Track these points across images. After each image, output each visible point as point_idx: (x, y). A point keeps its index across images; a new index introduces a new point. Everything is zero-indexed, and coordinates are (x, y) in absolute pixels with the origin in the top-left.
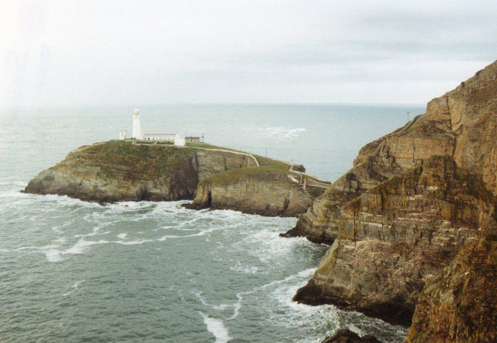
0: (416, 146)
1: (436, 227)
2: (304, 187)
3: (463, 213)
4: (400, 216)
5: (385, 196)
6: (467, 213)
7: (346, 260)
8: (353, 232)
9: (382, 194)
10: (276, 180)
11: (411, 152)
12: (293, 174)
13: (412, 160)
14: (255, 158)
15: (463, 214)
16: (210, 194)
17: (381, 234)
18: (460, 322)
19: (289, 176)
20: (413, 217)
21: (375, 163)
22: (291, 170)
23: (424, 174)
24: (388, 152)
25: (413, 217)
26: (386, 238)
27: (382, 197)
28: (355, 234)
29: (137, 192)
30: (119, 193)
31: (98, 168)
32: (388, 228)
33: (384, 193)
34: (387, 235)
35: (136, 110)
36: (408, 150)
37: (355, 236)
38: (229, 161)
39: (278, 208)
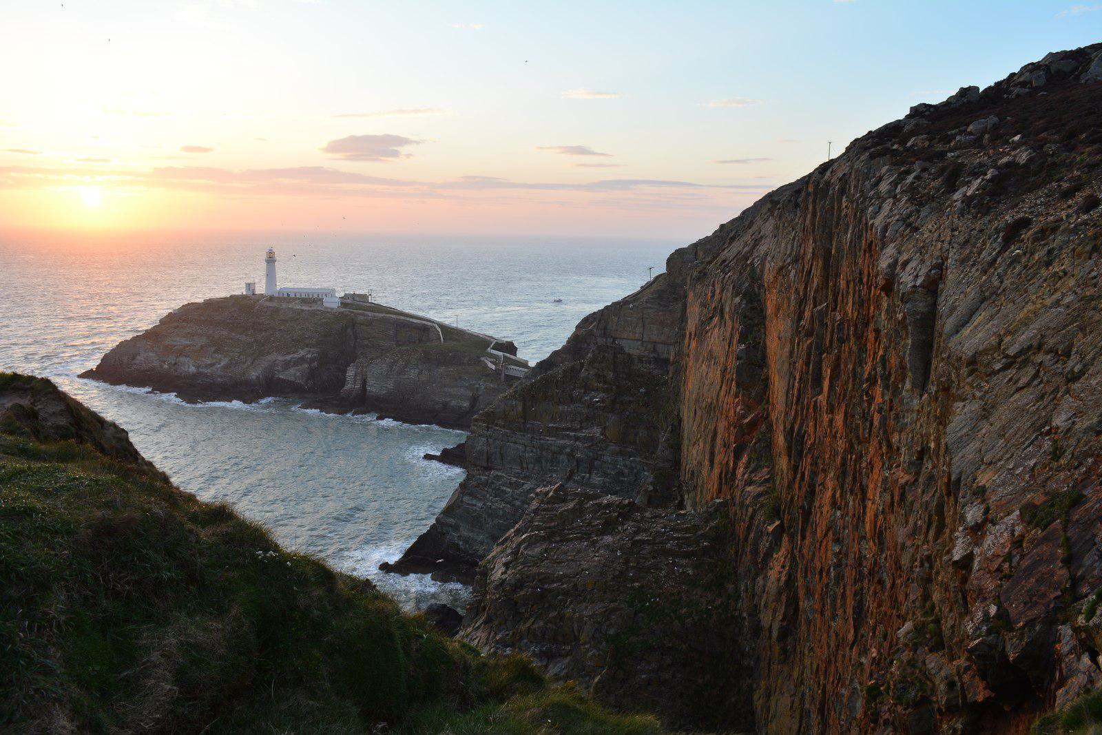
1: (599, 453)
4: (549, 436)
6: (642, 433)
7: (476, 497)
8: (485, 457)
11: (639, 330)
12: (491, 356)
13: (640, 343)
14: (439, 329)
16: (364, 383)
17: (523, 460)
18: (501, 609)
19: (482, 359)
20: (568, 437)
21: (586, 345)
23: (584, 373)
24: (605, 329)
25: (568, 437)
26: (531, 466)
28: (488, 459)
30: (231, 377)
32: (532, 451)
34: (531, 463)
36: (635, 327)
37: (487, 461)
39: (460, 407)
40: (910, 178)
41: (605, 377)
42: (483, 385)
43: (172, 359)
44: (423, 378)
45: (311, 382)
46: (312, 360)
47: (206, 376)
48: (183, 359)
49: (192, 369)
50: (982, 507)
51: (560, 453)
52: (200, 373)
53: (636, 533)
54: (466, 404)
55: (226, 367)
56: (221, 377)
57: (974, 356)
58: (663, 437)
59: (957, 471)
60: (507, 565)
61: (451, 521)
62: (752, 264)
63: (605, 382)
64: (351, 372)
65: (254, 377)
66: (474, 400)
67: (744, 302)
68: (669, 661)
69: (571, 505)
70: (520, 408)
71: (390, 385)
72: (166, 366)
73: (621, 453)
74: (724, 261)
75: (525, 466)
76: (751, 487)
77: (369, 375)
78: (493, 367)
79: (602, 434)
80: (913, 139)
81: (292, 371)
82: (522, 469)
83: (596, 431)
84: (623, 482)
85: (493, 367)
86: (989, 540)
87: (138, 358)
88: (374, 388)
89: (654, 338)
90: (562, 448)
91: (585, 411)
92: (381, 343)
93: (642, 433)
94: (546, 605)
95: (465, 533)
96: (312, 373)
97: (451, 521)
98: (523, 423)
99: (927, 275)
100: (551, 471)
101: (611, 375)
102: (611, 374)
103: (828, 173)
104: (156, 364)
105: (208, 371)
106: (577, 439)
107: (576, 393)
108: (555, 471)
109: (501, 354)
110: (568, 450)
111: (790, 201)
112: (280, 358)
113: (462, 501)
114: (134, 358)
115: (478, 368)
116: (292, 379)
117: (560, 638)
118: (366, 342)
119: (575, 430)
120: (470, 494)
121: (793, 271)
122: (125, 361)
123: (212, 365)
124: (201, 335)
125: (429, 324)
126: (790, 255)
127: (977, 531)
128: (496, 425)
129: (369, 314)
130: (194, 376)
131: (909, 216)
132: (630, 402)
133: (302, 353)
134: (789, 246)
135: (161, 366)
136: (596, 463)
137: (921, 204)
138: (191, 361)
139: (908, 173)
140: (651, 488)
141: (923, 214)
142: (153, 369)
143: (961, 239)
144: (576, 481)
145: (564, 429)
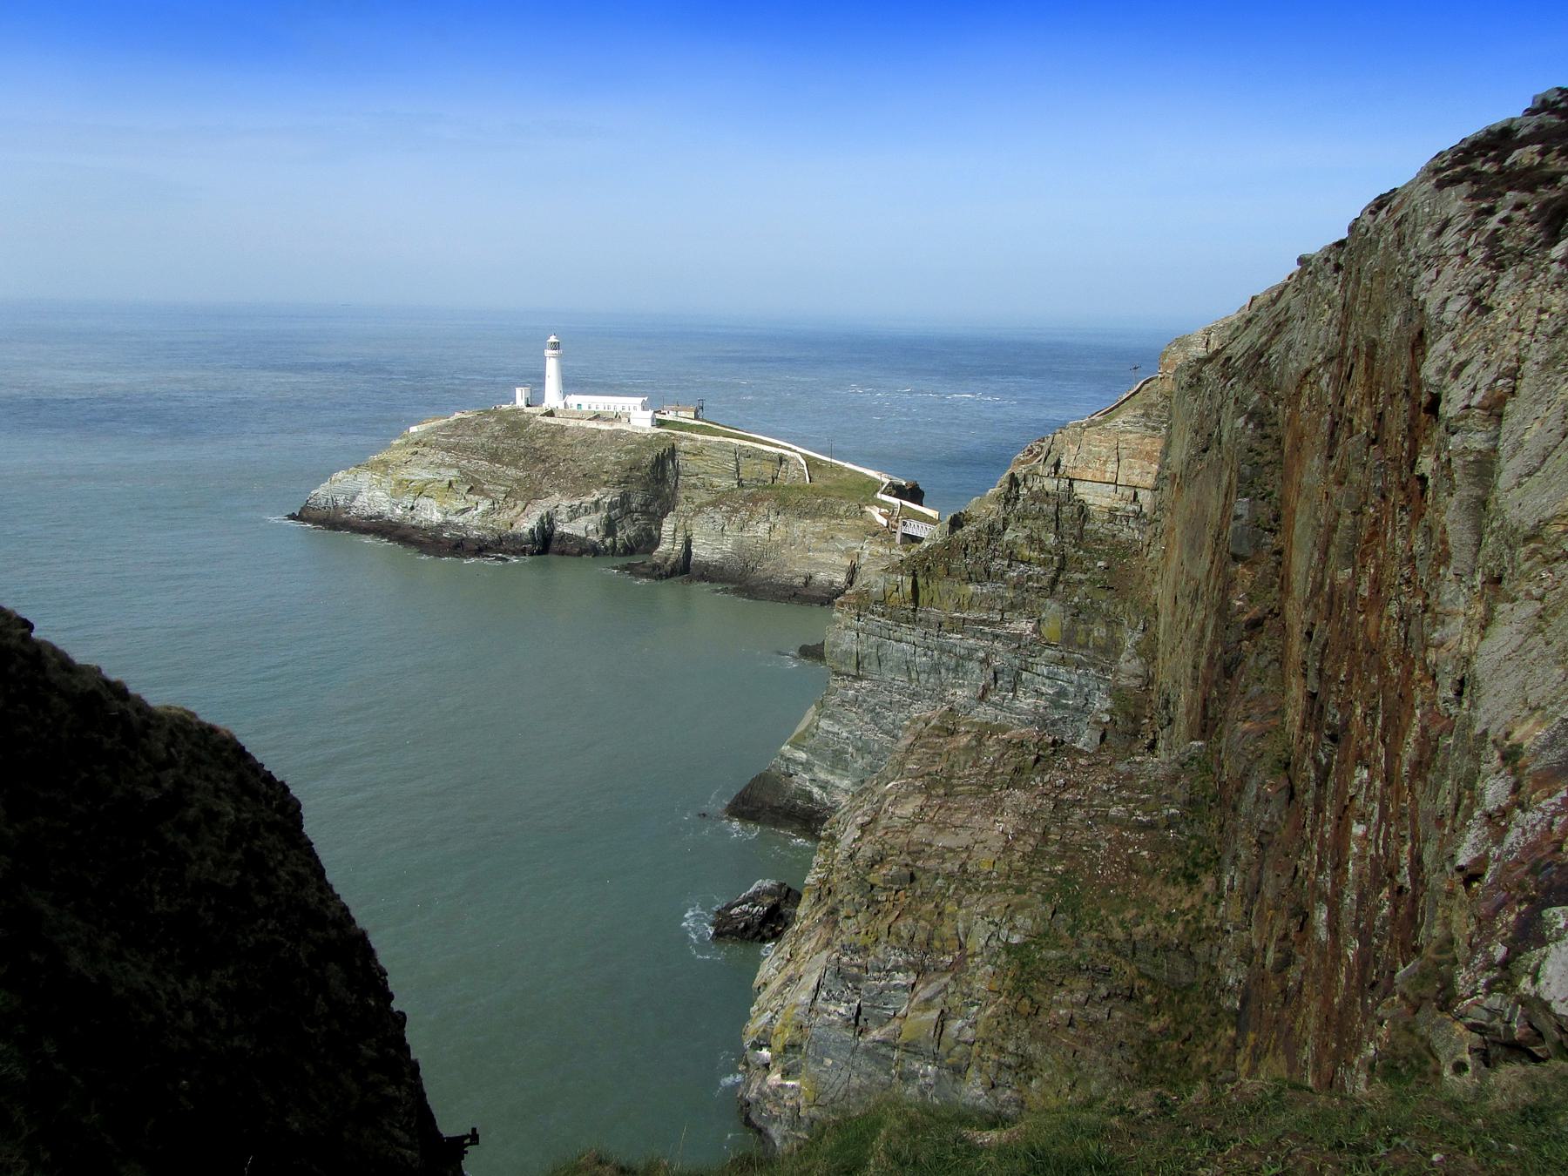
0: (1124, 453)
2: (898, 538)
3: (1088, 633)
5: (921, 581)
9: (914, 575)
10: (838, 516)
11: (1112, 467)
12: (881, 504)
15: (1088, 635)
16: (688, 543)
19: (867, 509)
22: (879, 495)
23: (1009, 536)
24: (1057, 465)
27: (915, 584)
29: (532, 531)
31: (455, 472)
33: (920, 573)
35: (553, 339)
36: (1105, 462)
38: (749, 469)
39: (831, 583)
40: (1493, 223)
41: (1041, 541)
42: (869, 550)
43: (408, 501)
44: (776, 537)
45: (608, 541)
46: (612, 506)
47: (456, 527)
48: (422, 501)
49: (437, 518)
50: (1512, 779)
51: (969, 657)
52: (448, 522)
53: (1066, 787)
54: (841, 579)
55: (485, 514)
56: (478, 528)
57: (1536, 527)
58: (1130, 639)
59: (1485, 719)
60: (863, 827)
61: (802, 756)
62: (1267, 364)
63: (1042, 550)
64: (668, 526)
65: (526, 531)
66: (853, 572)
67: (1251, 426)
68: (1103, 991)
69: (964, 740)
70: (909, 588)
71: (728, 546)
72: (399, 512)
73: (1063, 661)
74: (1229, 359)
75: (914, 675)
76: (1247, 725)
77: (696, 530)
78: (884, 522)
79: (1035, 631)
80: (1517, 152)
81: (582, 521)
82: (910, 680)
83: (1025, 626)
84: (1066, 707)
85: (884, 522)
86: (1511, 838)
87: (360, 498)
88: (702, 551)
89: (1136, 480)
90: (971, 652)
91: (1010, 594)
92: (716, 481)
93: (1099, 632)
94: (919, 892)
95: (822, 776)
96: (610, 527)
97: (802, 756)
98: (914, 610)
99: (1490, 388)
100: (953, 686)
101: (1050, 539)
102: (1052, 537)
103: (1383, 213)
104: (385, 508)
105: (460, 520)
106: (997, 636)
107: (996, 565)
108: (961, 686)
109: (896, 501)
110: (981, 655)
111: (1327, 260)
112: (566, 503)
113: (817, 727)
114: (354, 498)
115: (861, 523)
116: (583, 534)
117: (937, 944)
118: (693, 480)
119: (992, 624)
120: (830, 717)
121: (1327, 376)
122: (341, 503)
123: (464, 511)
124: (451, 466)
125: (788, 453)
126: (1322, 349)
127: (1497, 822)
128: (872, 612)
129: (699, 437)
130: (441, 527)
131: (1480, 287)
132: (1081, 582)
133: (597, 495)
134: (1321, 334)
135: (392, 511)
136: (1025, 675)
137: (1501, 267)
138: (435, 504)
139: (1490, 212)
140: (1107, 718)
141: (1503, 283)
142: (380, 516)
143: (1550, 329)
144: (995, 705)
145: (975, 622)
